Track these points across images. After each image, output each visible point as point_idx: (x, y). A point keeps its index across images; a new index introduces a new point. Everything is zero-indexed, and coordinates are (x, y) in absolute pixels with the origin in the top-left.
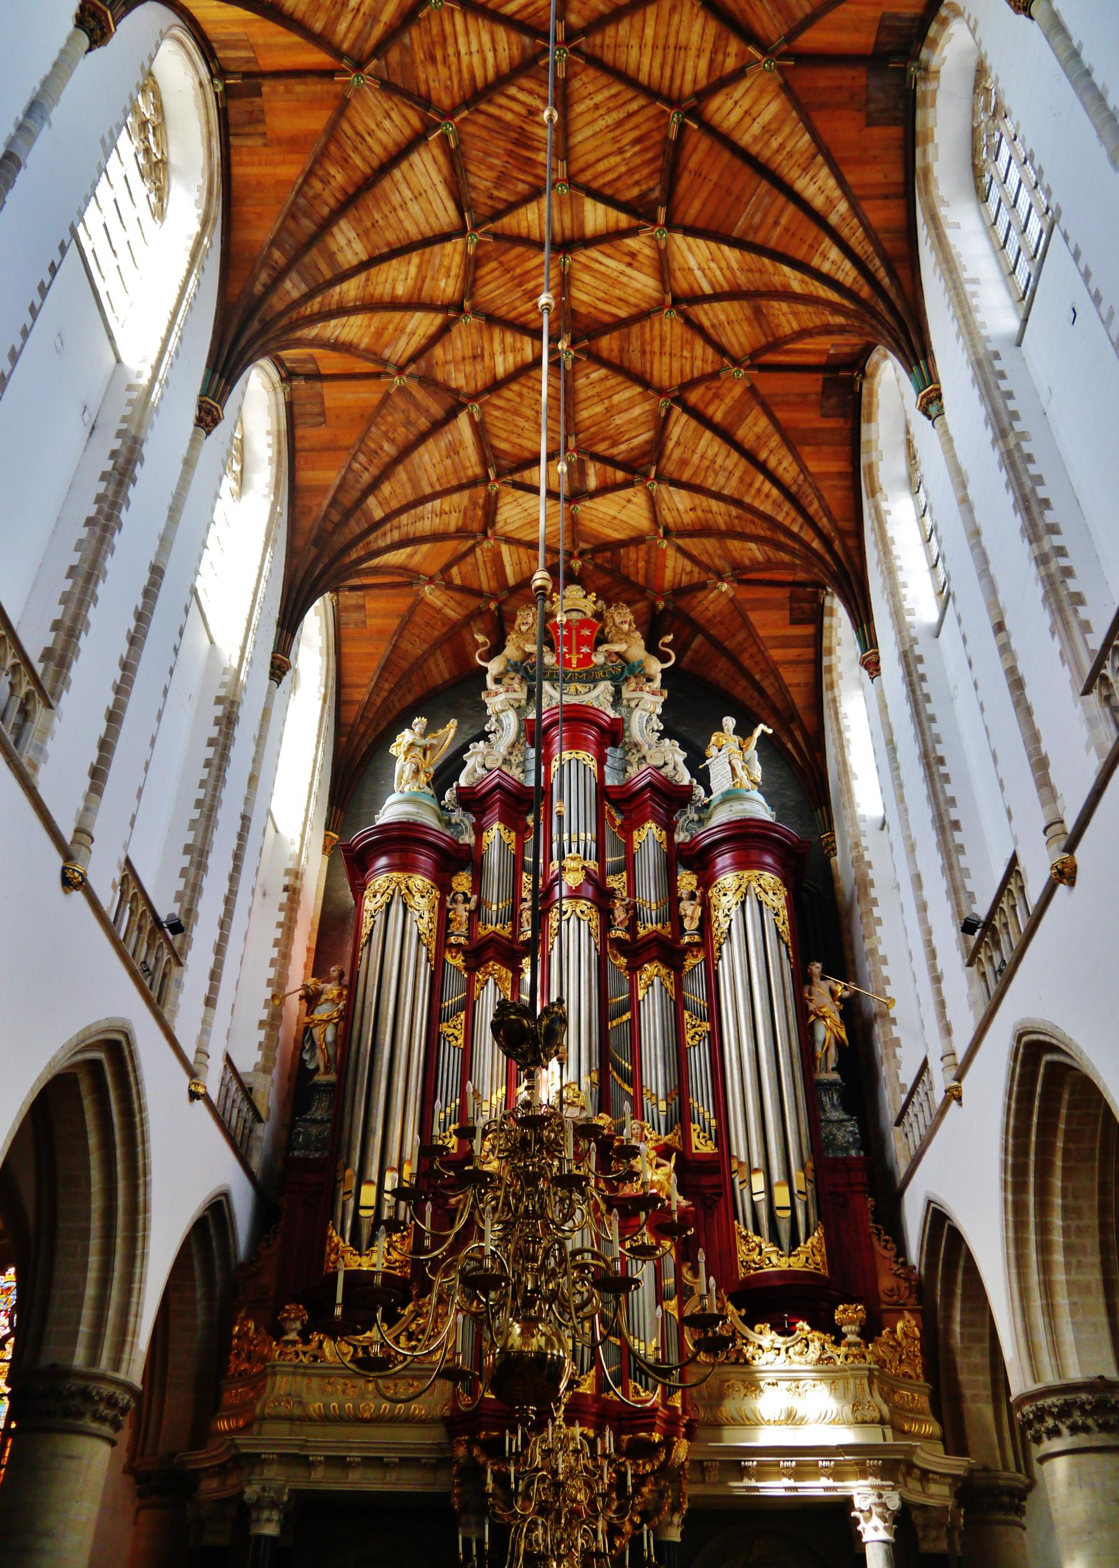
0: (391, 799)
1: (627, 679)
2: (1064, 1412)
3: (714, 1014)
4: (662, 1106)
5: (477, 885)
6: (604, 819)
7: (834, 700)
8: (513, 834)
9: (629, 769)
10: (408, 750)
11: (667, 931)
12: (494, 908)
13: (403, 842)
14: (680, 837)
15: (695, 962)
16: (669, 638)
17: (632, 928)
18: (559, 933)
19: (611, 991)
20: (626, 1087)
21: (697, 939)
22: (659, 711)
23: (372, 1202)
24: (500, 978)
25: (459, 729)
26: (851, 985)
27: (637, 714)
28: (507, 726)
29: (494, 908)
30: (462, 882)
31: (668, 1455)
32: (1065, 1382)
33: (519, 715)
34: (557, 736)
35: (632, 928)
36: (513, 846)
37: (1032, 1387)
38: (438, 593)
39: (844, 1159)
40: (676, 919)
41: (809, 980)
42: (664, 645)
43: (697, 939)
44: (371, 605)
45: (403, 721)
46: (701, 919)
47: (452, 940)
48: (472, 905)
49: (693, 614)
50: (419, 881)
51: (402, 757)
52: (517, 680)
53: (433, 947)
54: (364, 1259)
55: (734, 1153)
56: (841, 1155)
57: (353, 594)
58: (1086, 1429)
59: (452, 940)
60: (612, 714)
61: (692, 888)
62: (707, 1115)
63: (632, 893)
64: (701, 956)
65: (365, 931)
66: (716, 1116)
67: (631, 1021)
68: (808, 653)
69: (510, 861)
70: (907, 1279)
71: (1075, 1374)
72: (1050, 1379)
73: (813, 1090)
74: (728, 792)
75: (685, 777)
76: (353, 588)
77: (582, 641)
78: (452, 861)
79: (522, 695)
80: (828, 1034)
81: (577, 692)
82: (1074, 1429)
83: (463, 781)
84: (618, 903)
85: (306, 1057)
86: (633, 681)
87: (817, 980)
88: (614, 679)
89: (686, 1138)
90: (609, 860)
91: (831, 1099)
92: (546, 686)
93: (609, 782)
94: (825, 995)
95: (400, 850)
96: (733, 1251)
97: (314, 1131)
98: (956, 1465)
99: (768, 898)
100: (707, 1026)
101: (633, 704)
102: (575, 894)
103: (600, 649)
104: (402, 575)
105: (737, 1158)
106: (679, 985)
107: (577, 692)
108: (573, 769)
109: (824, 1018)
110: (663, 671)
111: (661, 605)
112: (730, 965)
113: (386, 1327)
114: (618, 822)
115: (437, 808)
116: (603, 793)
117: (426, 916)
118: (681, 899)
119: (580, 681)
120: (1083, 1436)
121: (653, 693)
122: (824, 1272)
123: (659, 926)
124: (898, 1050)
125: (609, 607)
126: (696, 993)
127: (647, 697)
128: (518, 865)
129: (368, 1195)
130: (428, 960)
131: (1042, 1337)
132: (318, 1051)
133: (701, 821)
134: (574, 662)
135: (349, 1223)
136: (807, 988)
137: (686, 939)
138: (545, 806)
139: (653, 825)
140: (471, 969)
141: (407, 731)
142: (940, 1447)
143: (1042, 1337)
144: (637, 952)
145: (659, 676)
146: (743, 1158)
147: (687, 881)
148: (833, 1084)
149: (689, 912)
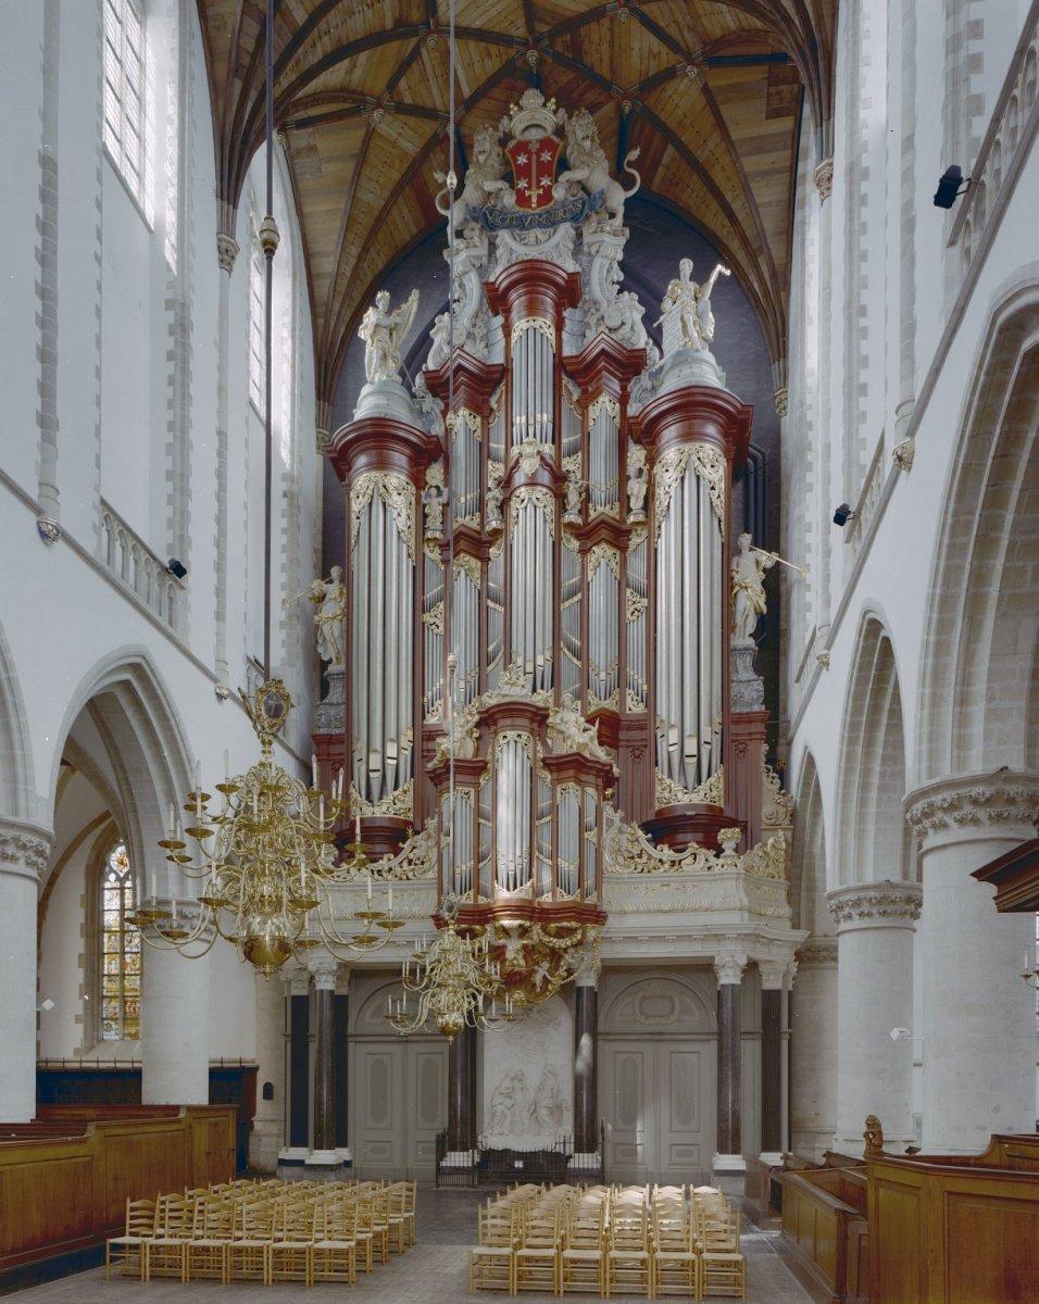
0: (366, 390)
1: (588, 217)
2: (857, 903)
3: (650, 591)
4: (603, 675)
5: (447, 481)
6: (560, 395)
7: (803, 223)
8: (479, 419)
9: (588, 332)
10: (375, 332)
11: (613, 512)
12: (463, 500)
13: (379, 434)
14: (633, 409)
15: (638, 540)
16: (634, 155)
17: (584, 511)
18: (516, 523)
19: (564, 575)
20: (575, 660)
21: (641, 518)
22: (620, 256)
23: (379, 766)
24: (470, 569)
25: (421, 300)
26: (775, 557)
27: (597, 262)
28: (468, 292)
29: (463, 500)
30: (434, 474)
31: (584, 934)
32: (861, 884)
33: (481, 276)
34: (517, 300)
35: (584, 511)
36: (479, 432)
37: (838, 888)
38: (389, 118)
39: (747, 714)
40: (624, 499)
41: (738, 552)
42: (630, 164)
43: (641, 518)
44: (322, 145)
45: (368, 300)
46: (646, 498)
47: (429, 535)
48: (443, 499)
49: (663, 116)
50: (397, 479)
51: (369, 342)
52: (477, 232)
53: (412, 542)
54: (376, 809)
55: (658, 712)
56: (746, 710)
57: (302, 132)
58: (869, 915)
59: (429, 535)
60: (571, 266)
61: (641, 465)
62: (640, 681)
63: (586, 474)
64: (645, 534)
65: (354, 532)
66: (648, 682)
67: (581, 601)
68: (783, 157)
69: (477, 449)
70: (785, 806)
71: (869, 879)
72: (852, 883)
73: (728, 652)
74: (679, 354)
75: (641, 340)
76: (301, 124)
77: (544, 169)
78: (427, 453)
79: (483, 251)
80: (749, 603)
81: (537, 241)
82: (861, 915)
83: (431, 364)
84: (571, 486)
85: (320, 650)
86: (594, 218)
87: (745, 551)
88: (574, 219)
89: (622, 702)
90: (565, 440)
91: (745, 662)
92: (504, 237)
93: (567, 351)
94: (751, 565)
95: (376, 448)
96: (652, 791)
97: (332, 711)
98: (801, 935)
99: (706, 472)
100: (645, 601)
101: (593, 251)
102: (532, 482)
103: (562, 178)
104: (345, 100)
105: (660, 716)
106: (623, 564)
107: (537, 241)
108: (529, 340)
109: (746, 588)
110: (627, 203)
111: (627, 106)
112: (666, 544)
113: (392, 856)
114: (575, 397)
115: (407, 397)
116: (561, 365)
117: (404, 514)
118: (629, 478)
119: (540, 225)
120: (867, 919)
121: (615, 234)
122: (721, 804)
123: (608, 506)
124: (808, 614)
125: (570, 117)
126: (637, 570)
127: (608, 239)
128: (484, 453)
129: (375, 761)
130: (409, 556)
131: (851, 854)
132: (329, 645)
133: (654, 389)
134: (534, 200)
135: (363, 783)
136: (735, 559)
137: (632, 519)
138: (507, 385)
139: (606, 399)
140: (446, 562)
141: (371, 310)
142: (788, 924)
143: (851, 854)
144: (587, 534)
145: (621, 210)
146: (664, 717)
147: (636, 455)
148: (746, 649)
149: (635, 491)
